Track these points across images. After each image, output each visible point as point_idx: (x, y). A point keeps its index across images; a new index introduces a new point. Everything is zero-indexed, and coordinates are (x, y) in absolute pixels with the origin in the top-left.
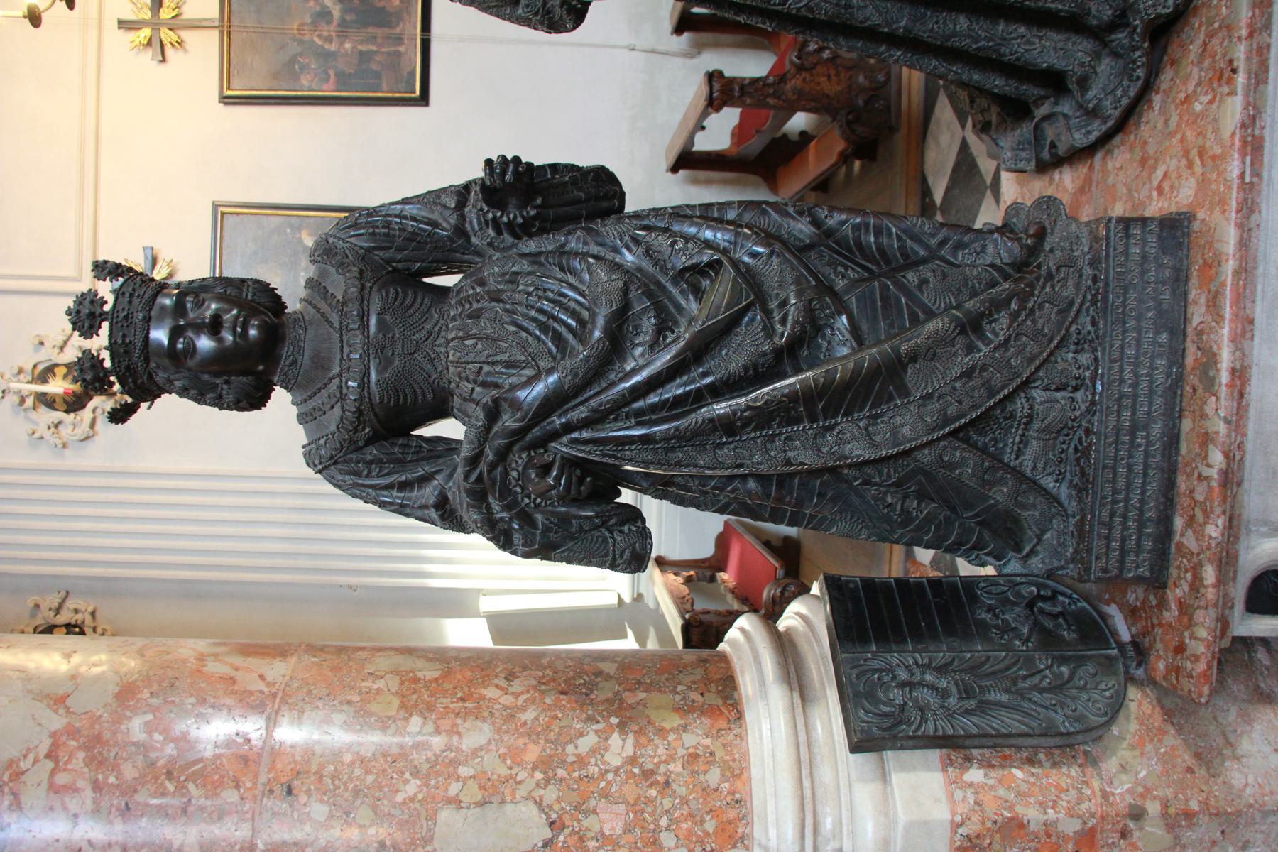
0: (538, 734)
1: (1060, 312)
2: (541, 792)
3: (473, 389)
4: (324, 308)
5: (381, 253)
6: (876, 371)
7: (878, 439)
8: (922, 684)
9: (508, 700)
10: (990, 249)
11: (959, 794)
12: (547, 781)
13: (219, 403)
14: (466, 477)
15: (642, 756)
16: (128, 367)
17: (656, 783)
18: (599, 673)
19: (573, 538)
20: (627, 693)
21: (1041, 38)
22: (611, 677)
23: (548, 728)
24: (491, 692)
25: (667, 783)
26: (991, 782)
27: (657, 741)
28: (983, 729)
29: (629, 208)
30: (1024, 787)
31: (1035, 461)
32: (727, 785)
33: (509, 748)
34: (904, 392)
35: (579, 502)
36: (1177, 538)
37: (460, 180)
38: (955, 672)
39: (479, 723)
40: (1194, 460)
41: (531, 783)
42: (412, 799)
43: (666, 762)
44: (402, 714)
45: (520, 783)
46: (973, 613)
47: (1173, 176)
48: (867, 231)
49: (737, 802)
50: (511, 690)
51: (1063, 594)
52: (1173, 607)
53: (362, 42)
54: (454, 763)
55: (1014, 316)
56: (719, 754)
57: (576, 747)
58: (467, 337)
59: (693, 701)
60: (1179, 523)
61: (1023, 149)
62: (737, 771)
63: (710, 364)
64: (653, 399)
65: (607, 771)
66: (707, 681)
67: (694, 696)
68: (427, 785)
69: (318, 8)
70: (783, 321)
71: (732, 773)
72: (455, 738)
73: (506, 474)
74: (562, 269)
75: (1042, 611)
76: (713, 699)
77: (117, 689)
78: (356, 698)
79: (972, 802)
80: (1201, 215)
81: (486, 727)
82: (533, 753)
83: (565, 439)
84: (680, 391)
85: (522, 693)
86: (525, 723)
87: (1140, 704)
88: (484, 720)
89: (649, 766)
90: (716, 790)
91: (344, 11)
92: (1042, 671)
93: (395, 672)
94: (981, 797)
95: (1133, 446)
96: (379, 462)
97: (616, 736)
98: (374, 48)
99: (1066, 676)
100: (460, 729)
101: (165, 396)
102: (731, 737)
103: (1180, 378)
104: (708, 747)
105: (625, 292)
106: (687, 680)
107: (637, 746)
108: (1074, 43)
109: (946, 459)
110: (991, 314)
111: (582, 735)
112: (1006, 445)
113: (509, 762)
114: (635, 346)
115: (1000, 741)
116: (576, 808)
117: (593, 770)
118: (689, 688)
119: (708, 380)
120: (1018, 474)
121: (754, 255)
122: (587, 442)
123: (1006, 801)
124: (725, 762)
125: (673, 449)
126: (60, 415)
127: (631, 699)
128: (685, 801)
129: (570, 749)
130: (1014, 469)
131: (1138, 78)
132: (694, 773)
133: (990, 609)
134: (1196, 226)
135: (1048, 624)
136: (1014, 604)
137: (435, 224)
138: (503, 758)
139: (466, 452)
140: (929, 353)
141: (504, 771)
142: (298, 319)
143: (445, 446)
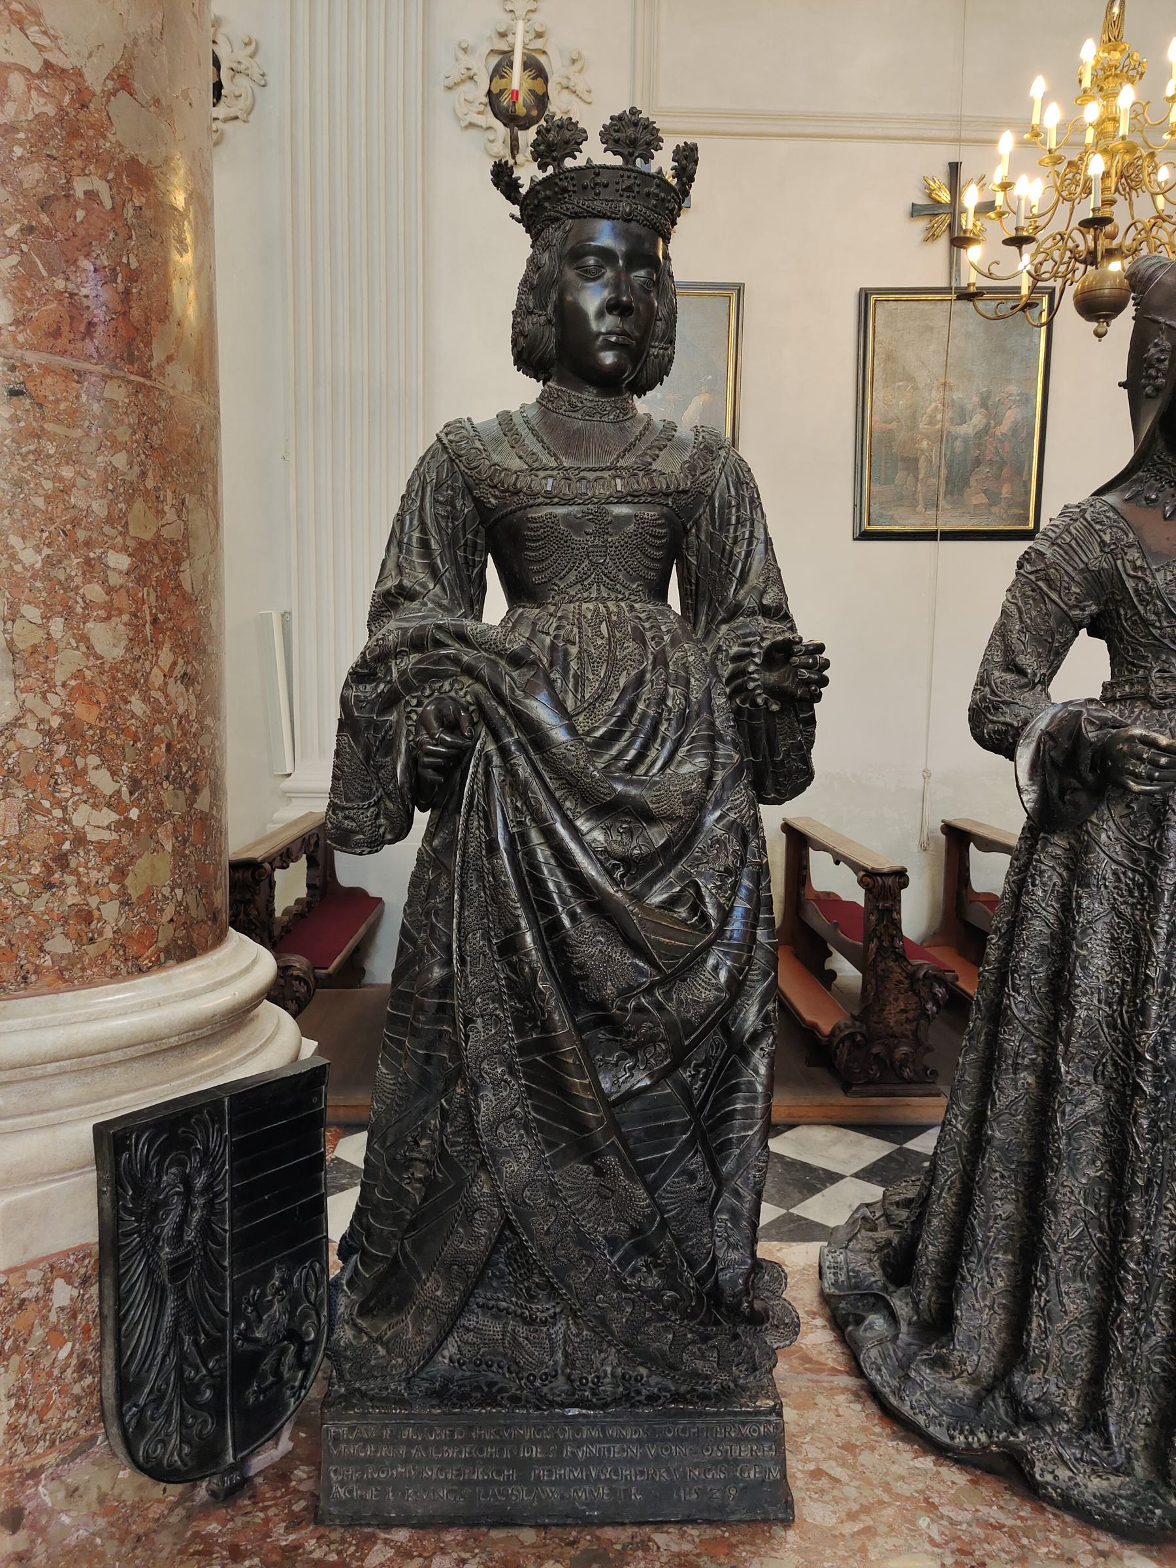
0: (113, 718)
1: (663, 1354)
2: (32, 726)
3: (548, 634)
4: (642, 447)
5: (707, 516)
7: (501, 1131)
9: (157, 678)
10: (734, 1255)
11: (34, 1275)
12: (49, 733)
13: (521, 312)
14: (439, 627)
15: (87, 852)
16: (565, 190)
17: (50, 871)
18: (196, 790)
19: (368, 757)
20: (170, 826)
21: (991, 1308)
22: (191, 806)
23: (121, 731)
24: (166, 656)
25: (49, 886)
26: (53, 1317)
27: (108, 869)
28: (127, 1299)
30: (45, 1363)
31: (476, 1330)
32: (49, 963)
33: (91, 684)
35: (413, 763)
36: (383, 1535)
37: (794, 609)
38: (204, 1249)
39: (124, 643)
40: (483, 1550)
41: (44, 712)
42: (13, 557)
43: (79, 883)
44: (132, 544)
45: (44, 698)
46: (280, 1261)
47: (836, 1493)
48: (747, 1100)
49: (25, 978)
50: (171, 681)
51: (305, 1378)
52: (292, 1537)
53: (929, 461)
54: (68, 613)
55: (656, 1295)
56: (92, 949)
57: (96, 768)
58: (612, 626)
59: (162, 910)
60: (401, 1535)
61: (849, 1277)
62: (69, 975)
63: (587, 920)
65: (65, 809)
66: (189, 925)
67: (170, 911)
68: (34, 577)
69: (969, 407)
71: (66, 969)
72: (103, 614)
74: (693, 740)
75: (284, 1351)
76: (165, 936)
77: (144, 162)
78: (150, 483)
79: (24, 1296)
80: (791, 1535)
81: (119, 652)
82: (85, 713)
83: (491, 747)
84: (551, 886)
85: (167, 696)
86: (127, 702)
87: (159, 1501)
88: (128, 649)
89: (73, 863)
90: (41, 950)
91: (966, 441)
92: (206, 1365)
94: (31, 1307)
96: (452, 516)
97: (114, 817)
98: (921, 476)
99: (198, 1399)
100: (115, 620)
101: (528, 239)
102: (116, 963)
103: (587, 1523)
104: (101, 934)
106: (190, 899)
107: (101, 846)
108: (988, 1351)
109: (477, 1216)
110: (656, 1266)
111: (114, 773)
112: (496, 1290)
113: (73, 683)
114: (606, 830)
115: (110, 1323)
116: (10, 771)
117: (65, 791)
118: (180, 904)
119: (566, 922)
120: (462, 1308)
121: (716, 968)
122: (488, 775)
123: (25, 1342)
124: (80, 958)
125: (481, 878)
126: (484, 84)
128: (25, 911)
129: (94, 760)
130: (467, 1304)
131: (952, 1438)
132: (64, 920)
133: (286, 1283)
134: (777, 1530)
136: (292, 1314)
137: (743, 580)
138: (78, 675)
139: (469, 624)
141: (59, 678)
142: (627, 412)
143: (475, 603)
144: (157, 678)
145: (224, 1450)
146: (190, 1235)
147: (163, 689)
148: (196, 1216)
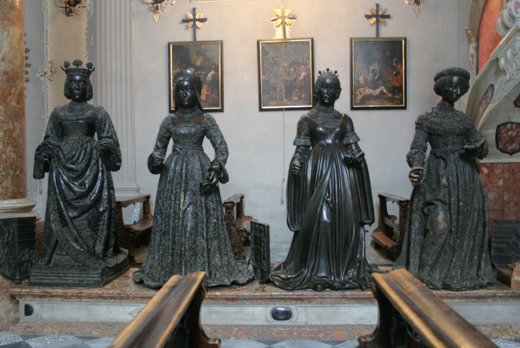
6: (66, 220)
8: (9, 235)
9: (8, 152)
10: (99, 248)
24: (10, 148)
29: (112, 172)
34: (63, 226)
64: (61, 178)
66: (15, 193)
67: (10, 190)
70: (75, 202)
73: (47, 150)
75: (28, 264)
76: (10, 194)
93: (14, 128)
95: (56, 276)
96: (55, 123)
105: (78, 171)
106: (15, 189)
121: (91, 197)
127: (9, 177)
133: (28, 252)
135: (25, 264)
137: (103, 131)
140: (70, 232)
144: (8, 152)
145: (16, 276)
146: (10, 239)
147: (9, 153)
148: (11, 236)
